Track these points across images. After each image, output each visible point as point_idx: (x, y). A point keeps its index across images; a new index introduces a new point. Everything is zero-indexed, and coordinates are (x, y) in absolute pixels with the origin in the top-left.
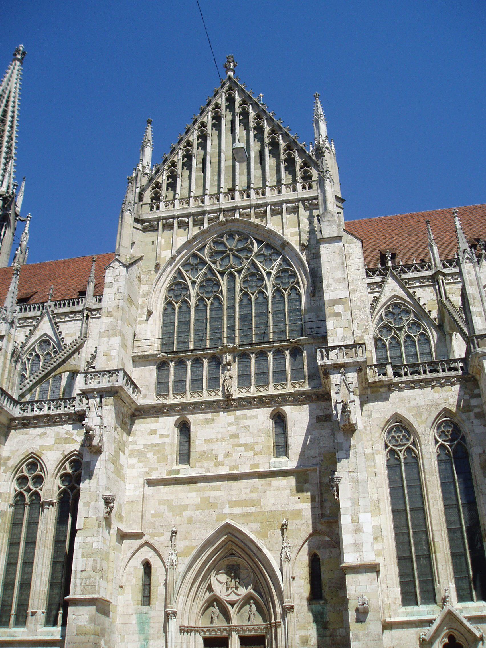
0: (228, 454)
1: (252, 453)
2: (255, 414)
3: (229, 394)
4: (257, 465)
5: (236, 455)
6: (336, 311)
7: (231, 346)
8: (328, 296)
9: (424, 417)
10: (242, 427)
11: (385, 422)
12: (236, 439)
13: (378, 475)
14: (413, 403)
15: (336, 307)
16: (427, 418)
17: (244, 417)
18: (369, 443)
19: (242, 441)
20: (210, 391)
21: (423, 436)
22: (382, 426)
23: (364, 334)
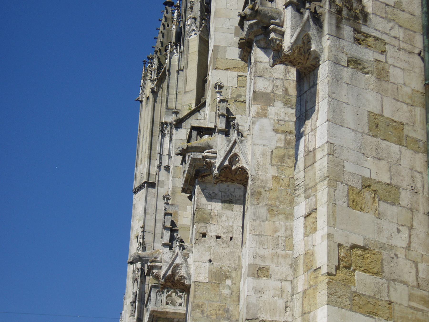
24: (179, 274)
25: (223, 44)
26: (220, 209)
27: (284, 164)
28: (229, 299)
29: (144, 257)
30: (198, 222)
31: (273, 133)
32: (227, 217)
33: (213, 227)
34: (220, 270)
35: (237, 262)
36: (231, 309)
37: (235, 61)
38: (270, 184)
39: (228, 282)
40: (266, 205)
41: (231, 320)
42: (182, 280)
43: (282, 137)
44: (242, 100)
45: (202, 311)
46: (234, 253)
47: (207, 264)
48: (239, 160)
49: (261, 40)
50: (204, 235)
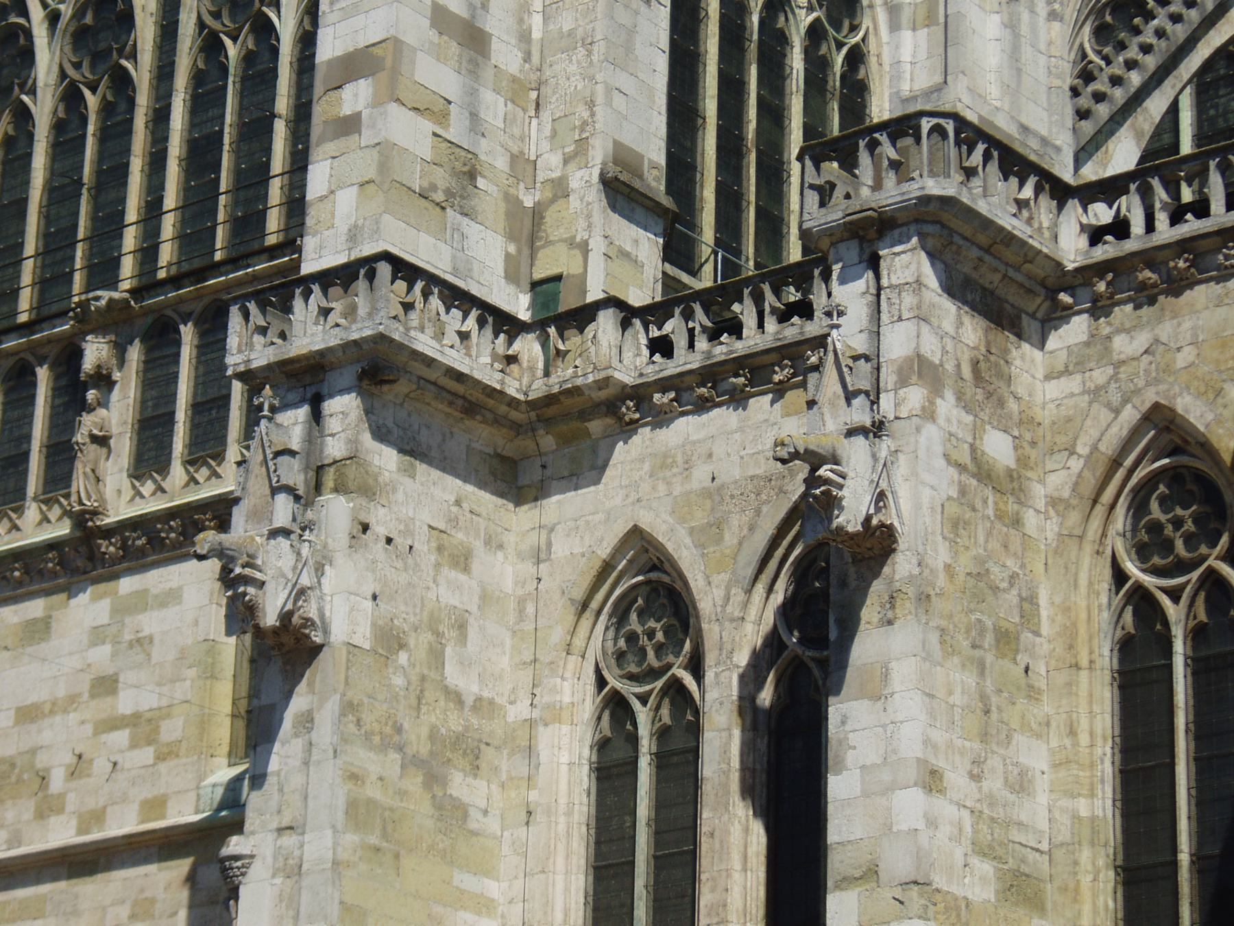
0: (79, 765)
1: (146, 755)
2: (174, 585)
3: (84, 512)
4: (156, 805)
5: (101, 766)
6: (347, 110)
7: (103, 302)
8: (328, 48)
9: (730, 539)
10: (131, 645)
11: (594, 572)
12: (109, 699)
13: (539, 817)
14: (701, 475)
15: (348, 91)
16: (740, 544)
17: (140, 603)
18: (526, 676)
19: (126, 703)
20: (46, 502)
21: (716, 628)
22: (579, 594)
23: (572, 167)
24: (302, 611)
25: (409, 39)
26: (394, 470)
27: (959, 540)
28: (403, 701)
29: (228, 549)
30: (356, 492)
31: (943, 462)
32: (405, 494)
33: (382, 512)
34: (390, 623)
35: (418, 611)
36: (406, 726)
37: (429, 92)
38: (942, 581)
39: (403, 658)
40: (938, 627)
41: (404, 754)
42: (305, 628)
43: (953, 471)
44: (438, 201)
45: (358, 721)
46: (414, 587)
47: (369, 604)
48: (885, 506)
49: (933, 236)
50: (365, 528)
